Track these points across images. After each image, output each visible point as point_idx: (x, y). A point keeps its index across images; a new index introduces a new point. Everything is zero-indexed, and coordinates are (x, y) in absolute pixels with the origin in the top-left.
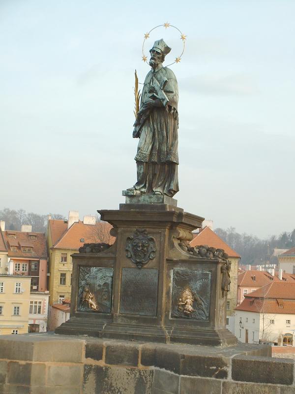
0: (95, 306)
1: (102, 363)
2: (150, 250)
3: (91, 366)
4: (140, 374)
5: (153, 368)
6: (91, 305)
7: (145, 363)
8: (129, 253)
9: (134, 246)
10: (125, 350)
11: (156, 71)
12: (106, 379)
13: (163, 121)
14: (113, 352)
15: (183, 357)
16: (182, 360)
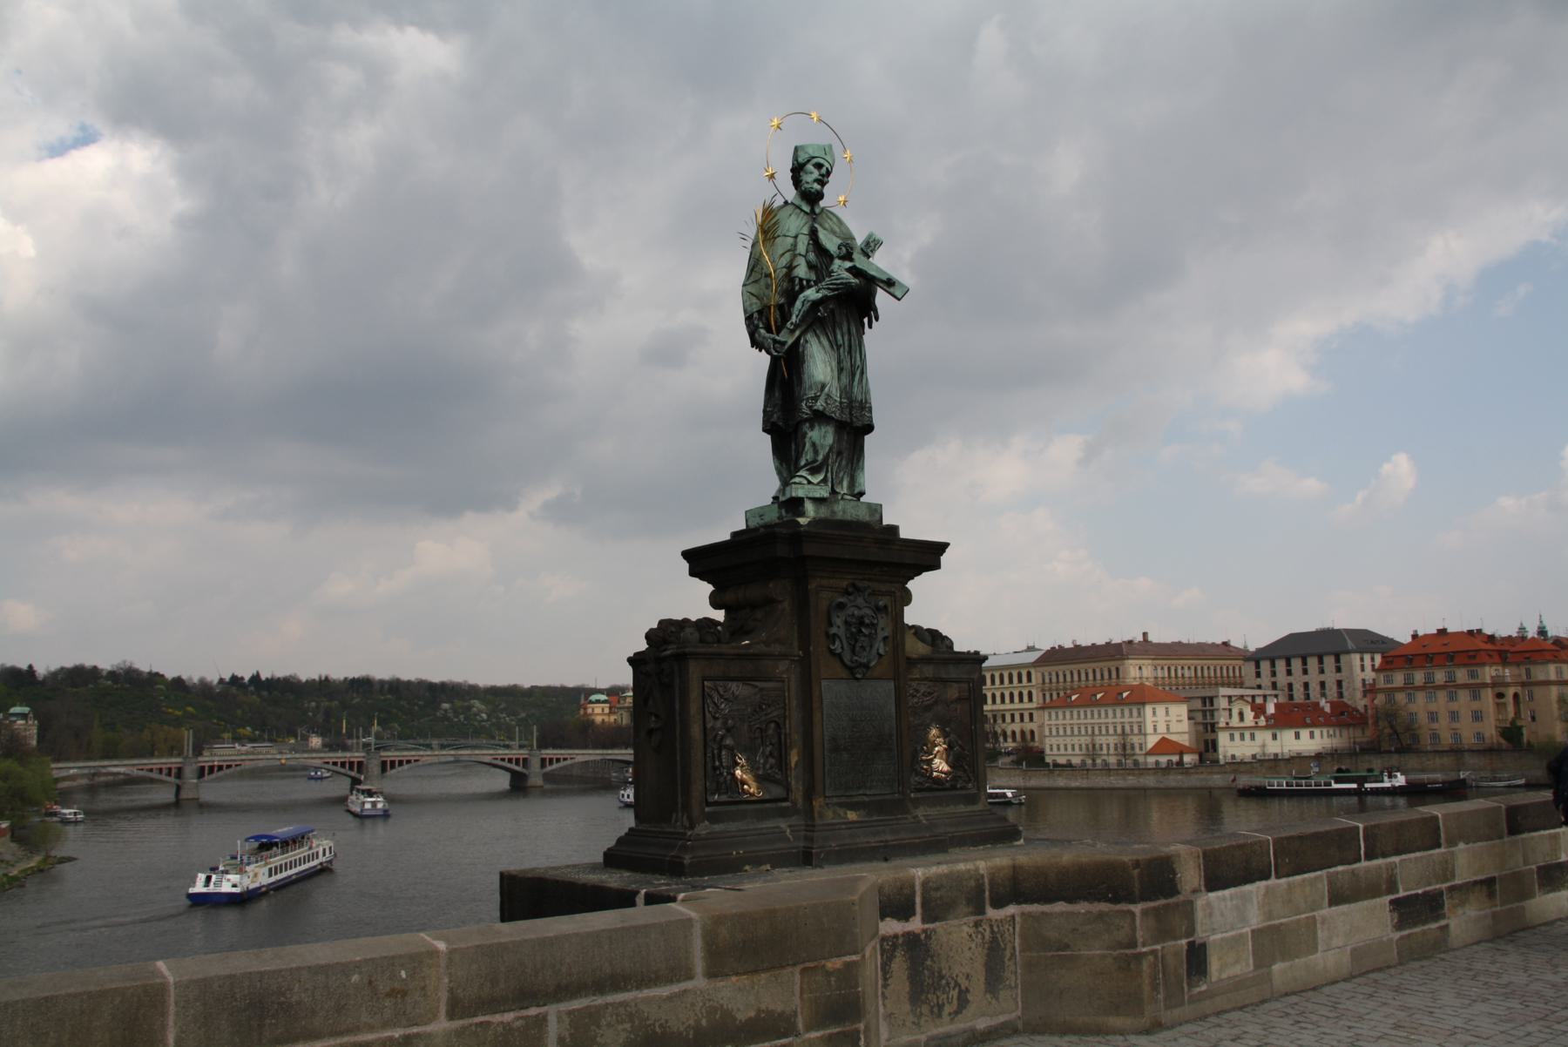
0: (752, 788)
1: (915, 924)
2: (881, 635)
3: (896, 936)
4: (992, 932)
5: (1011, 909)
6: (743, 783)
7: (998, 903)
8: (837, 643)
9: (846, 622)
10: (957, 879)
11: (817, 211)
12: (929, 962)
13: (854, 330)
14: (937, 889)
15: (1137, 864)
16: (1136, 872)
